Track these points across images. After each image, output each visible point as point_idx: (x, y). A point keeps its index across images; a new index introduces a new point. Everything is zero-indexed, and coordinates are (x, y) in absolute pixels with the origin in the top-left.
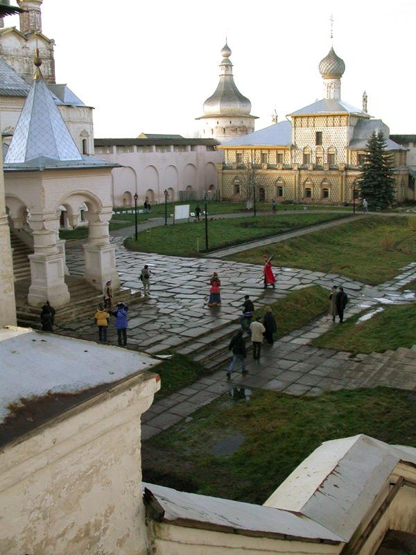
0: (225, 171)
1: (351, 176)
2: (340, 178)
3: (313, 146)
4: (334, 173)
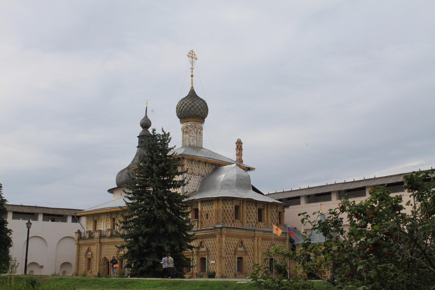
0: (81, 242)
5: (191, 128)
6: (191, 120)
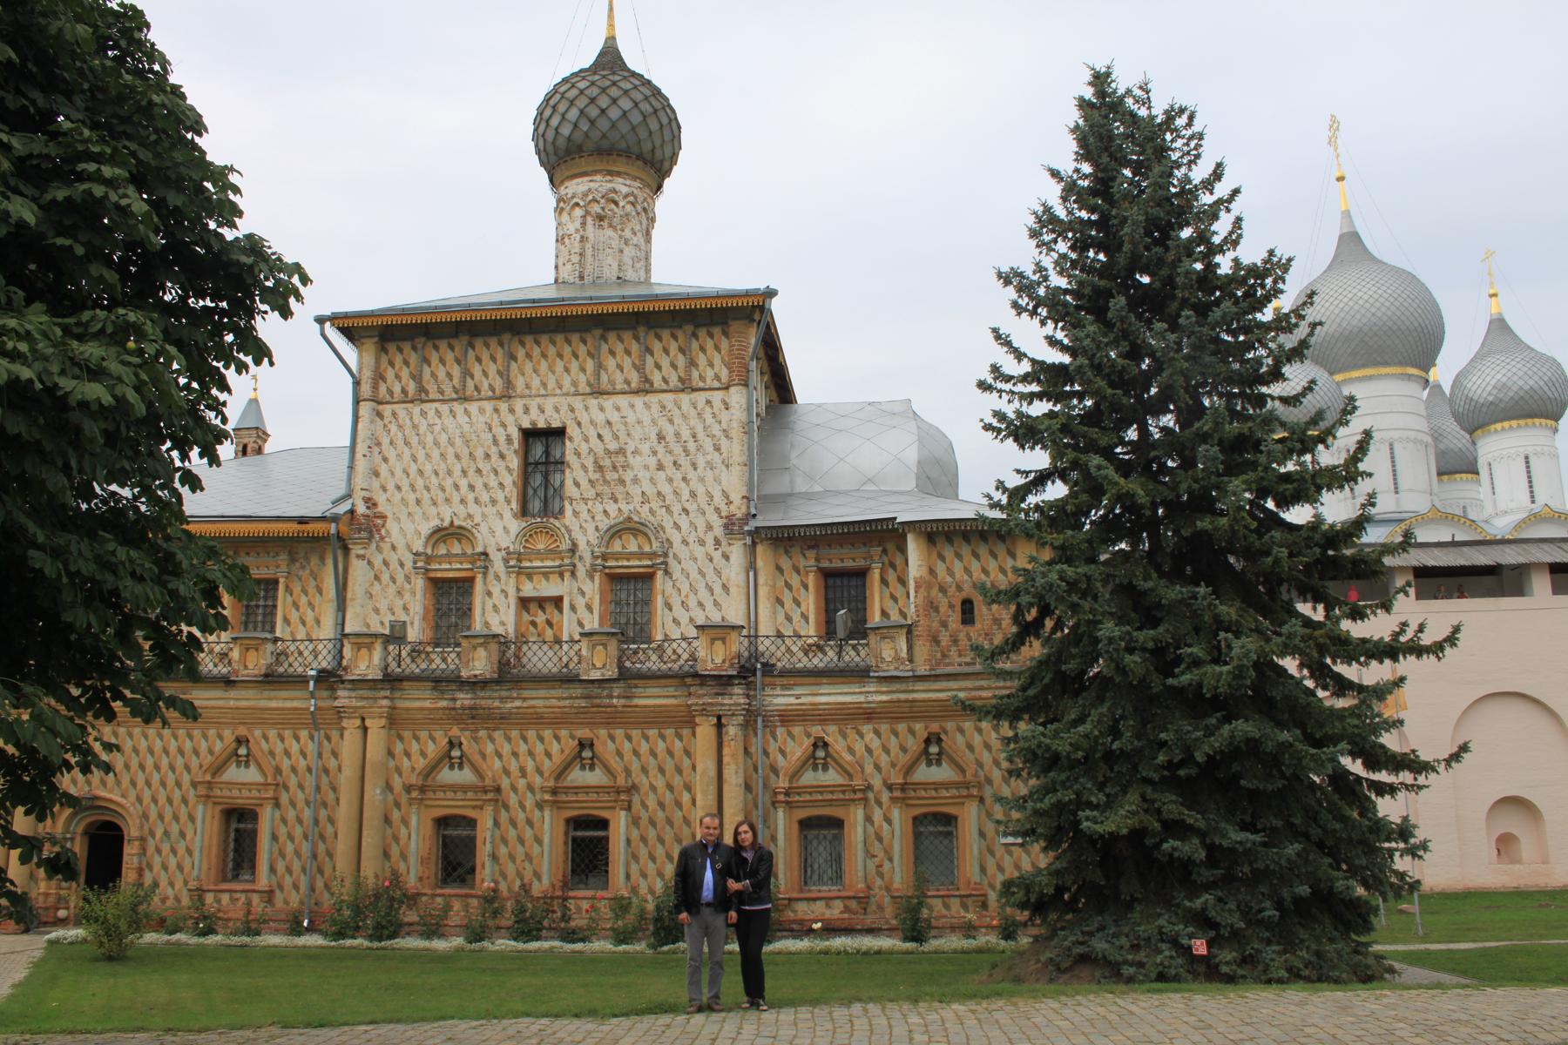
1: (788, 718)
2: (705, 730)
3: (499, 529)
4: (652, 698)
5: (629, 208)
6: (629, 169)
